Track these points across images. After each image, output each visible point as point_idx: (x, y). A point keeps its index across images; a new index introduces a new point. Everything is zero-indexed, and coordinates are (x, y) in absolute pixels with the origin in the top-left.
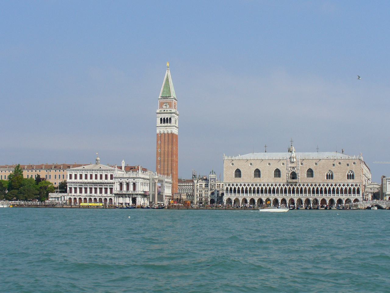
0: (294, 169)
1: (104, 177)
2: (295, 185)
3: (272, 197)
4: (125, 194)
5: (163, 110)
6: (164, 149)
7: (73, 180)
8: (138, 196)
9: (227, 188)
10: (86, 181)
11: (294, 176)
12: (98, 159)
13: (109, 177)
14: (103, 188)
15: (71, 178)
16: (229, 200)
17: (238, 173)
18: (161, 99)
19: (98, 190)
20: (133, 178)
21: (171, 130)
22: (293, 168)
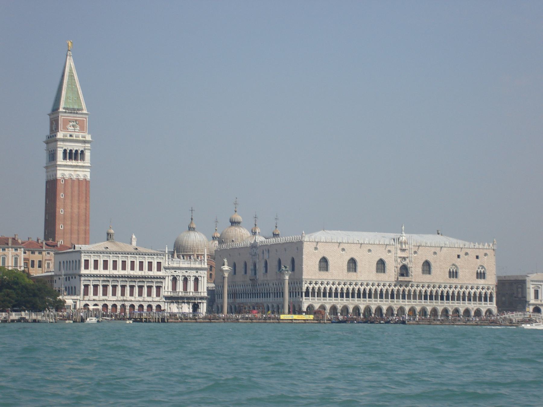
0: (405, 260)
1: (146, 265)
4: (182, 298)
6: (71, 209)
7: (91, 271)
8: (204, 301)
9: (307, 288)
10: (115, 272)
12: (112, 231)
13: (155, 265)
15: (87, 267)
17: (324, 264)
18: (65, 112)
19: (136, 290)
22: (404, 258)
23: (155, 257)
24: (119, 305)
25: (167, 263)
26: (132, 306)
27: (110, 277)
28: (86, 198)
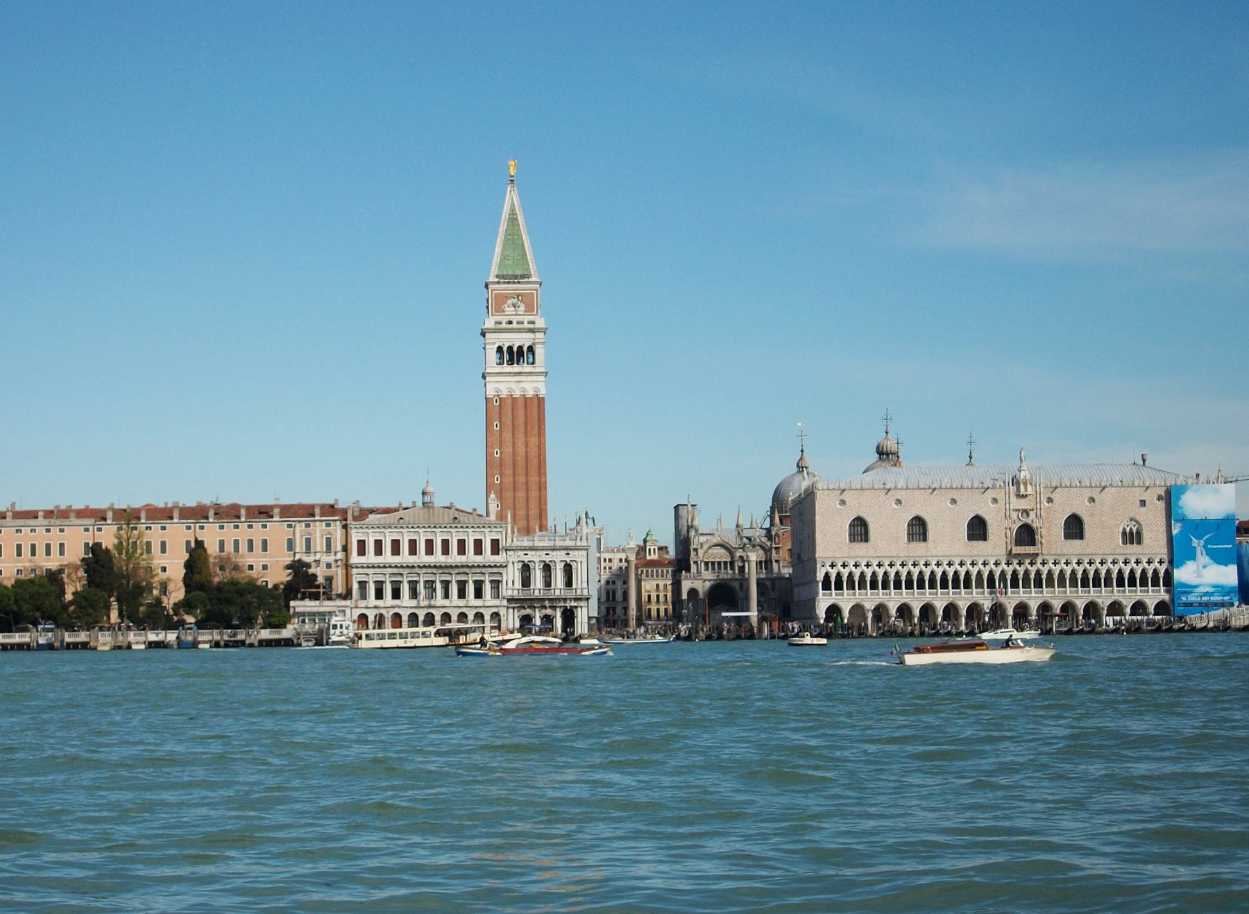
0: (1028, 515)
1: (470, 546)
2: (1032, 564)
3: (963, 600)
5: (504, 319)
7: (371, 557)
8: (583, 604)
10: (412, 560)
11: (1026, 535)
13: (487, 546)
15: (362, 552)
16: (834, 611)
17: (860, 529)
20: (566, 548)
22: (1026, 512)
25: (509, 540)
28: (539, 427)
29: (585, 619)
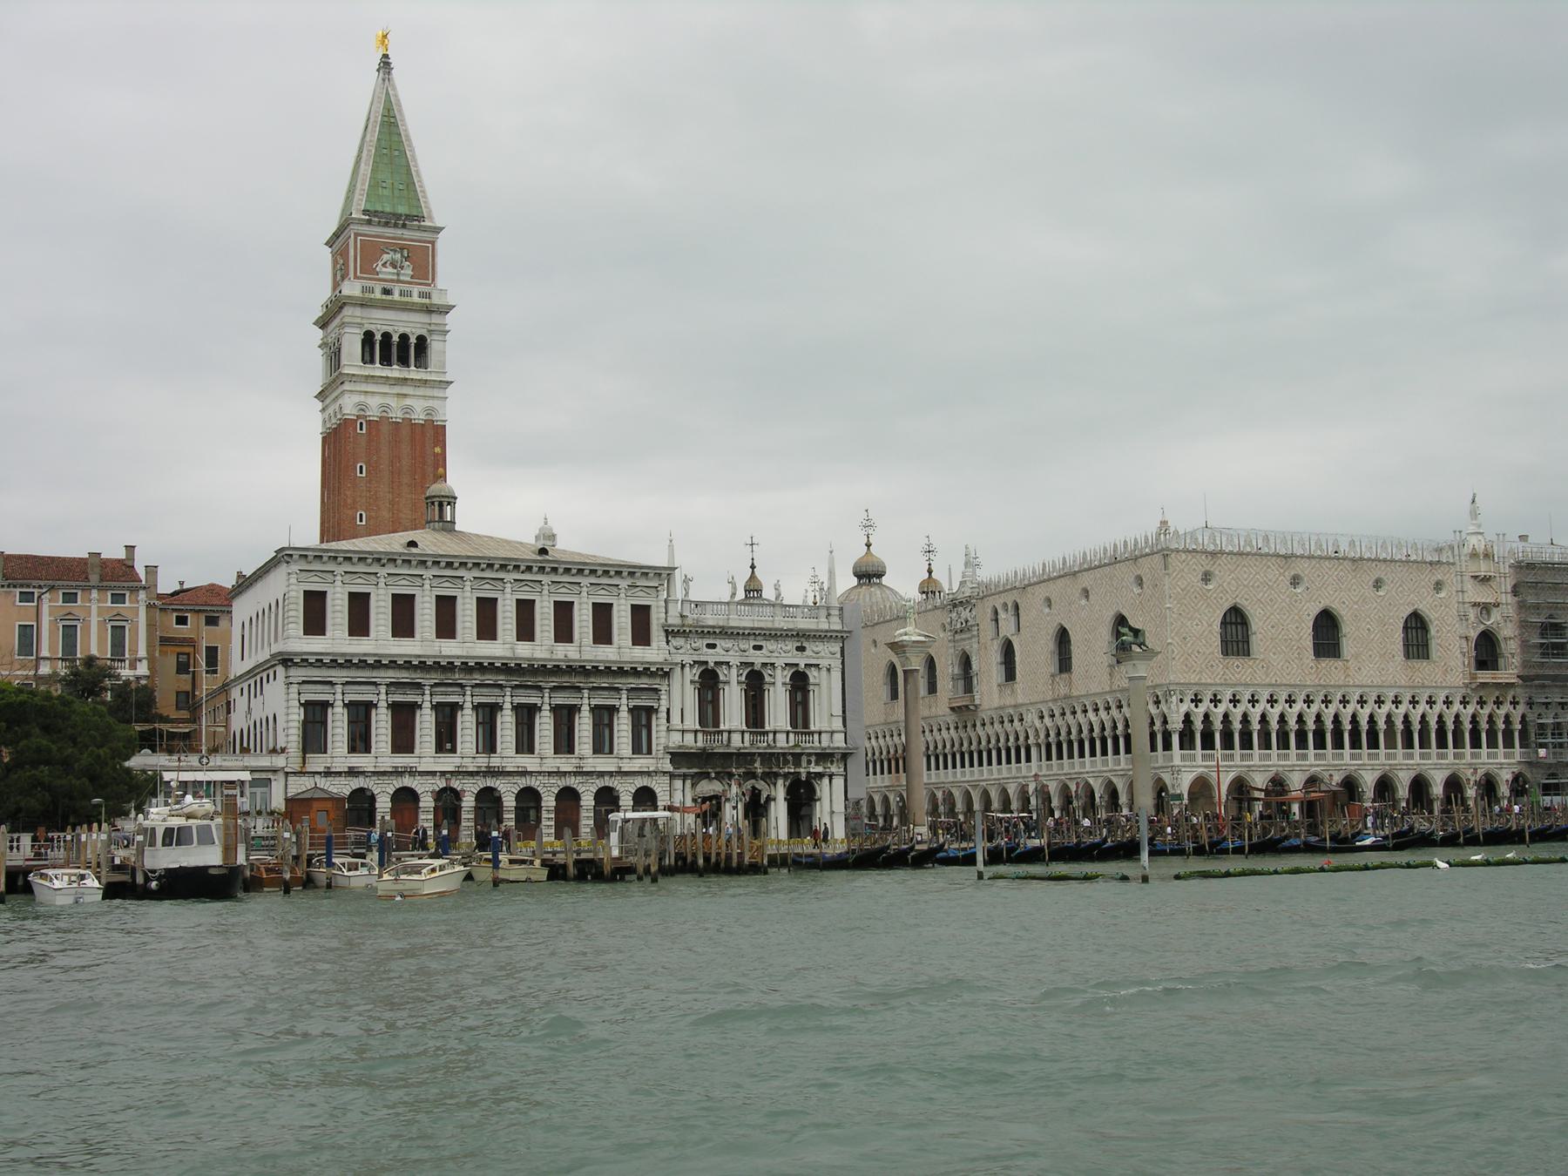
0: (1489, 613)
1: (583, 620)
4: (743, 758)
9: (1187, 715)
10: (449, 649)
11: (1487, 650)
13: (622, 621)
14: (585, 709)
17: (1236, 630)
19: (545, 726)
21: (430, 403)
22: (1486, 608)
23: (624, 583)
24: (469, 790)
26: (529, 797)
27: (423, 666)
29: (839, 806)
